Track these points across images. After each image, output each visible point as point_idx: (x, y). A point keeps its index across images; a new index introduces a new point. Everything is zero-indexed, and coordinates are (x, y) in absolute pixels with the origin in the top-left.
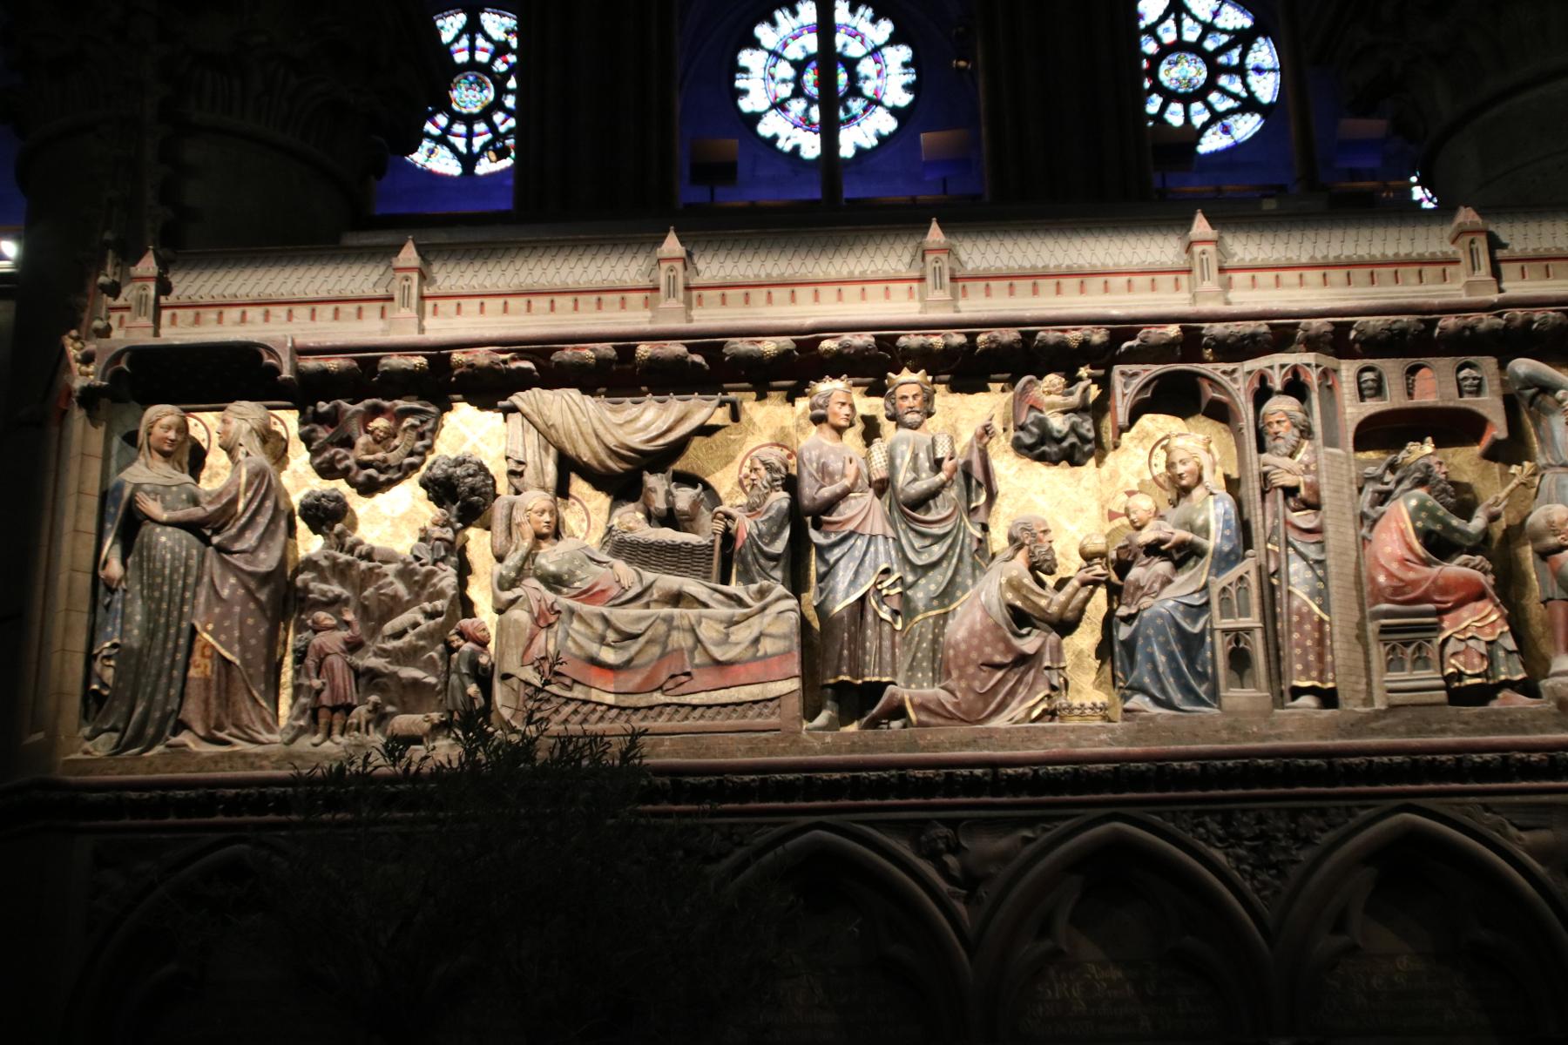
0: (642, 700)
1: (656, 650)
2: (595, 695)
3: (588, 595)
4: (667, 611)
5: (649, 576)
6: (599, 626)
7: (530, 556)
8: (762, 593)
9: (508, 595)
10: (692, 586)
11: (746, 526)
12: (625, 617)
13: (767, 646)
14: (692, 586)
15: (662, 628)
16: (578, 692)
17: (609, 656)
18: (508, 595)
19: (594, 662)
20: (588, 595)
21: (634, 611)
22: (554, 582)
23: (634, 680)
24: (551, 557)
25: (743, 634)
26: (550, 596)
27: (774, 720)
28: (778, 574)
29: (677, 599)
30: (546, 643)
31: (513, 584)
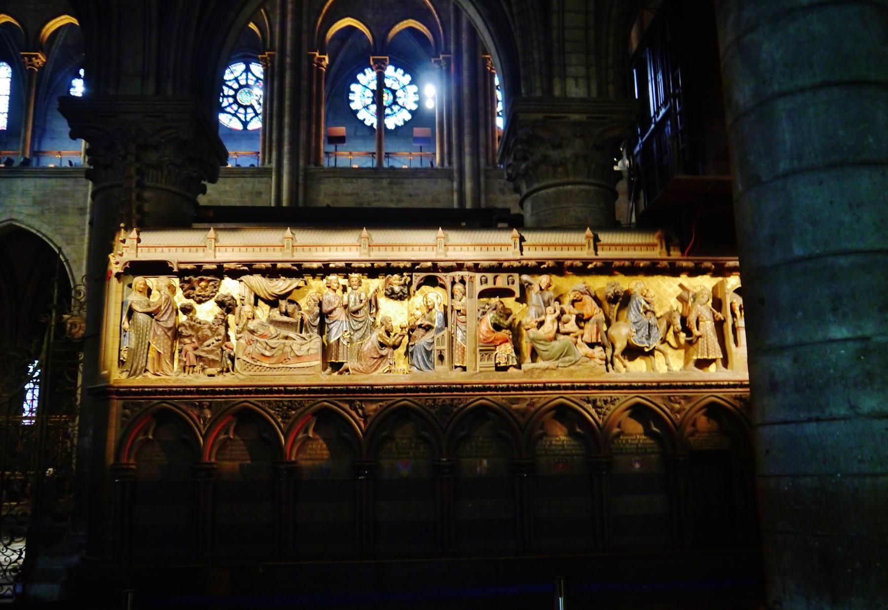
0: (276, 366)
1: (280, 352)
2: (263, 364)
3: (262, 336)
4: (284, 341)
5: (279, 330)
6: (265, 345)
7: (246, 324)
8: (310, 337)
9: (239, 336)
10: (292, 334)
11: (307, 317)
12: (272, 343)
13: (311, 352)
14: (292, 334)
15: (282, 346)
16: (259, 363)
17: (267, 353)
18: (239, 336)
19: (263, 355)
20: (262, 336)
21: (275, 341)
22: (252, 332)
23: (273, 360)
24: (252, 325)
25: (305, 348)
26: (251, 336)
27: (313, 372)
28: (316, 330)
29: (287, 338)
30: (250, 349)
31: (240, 332)
